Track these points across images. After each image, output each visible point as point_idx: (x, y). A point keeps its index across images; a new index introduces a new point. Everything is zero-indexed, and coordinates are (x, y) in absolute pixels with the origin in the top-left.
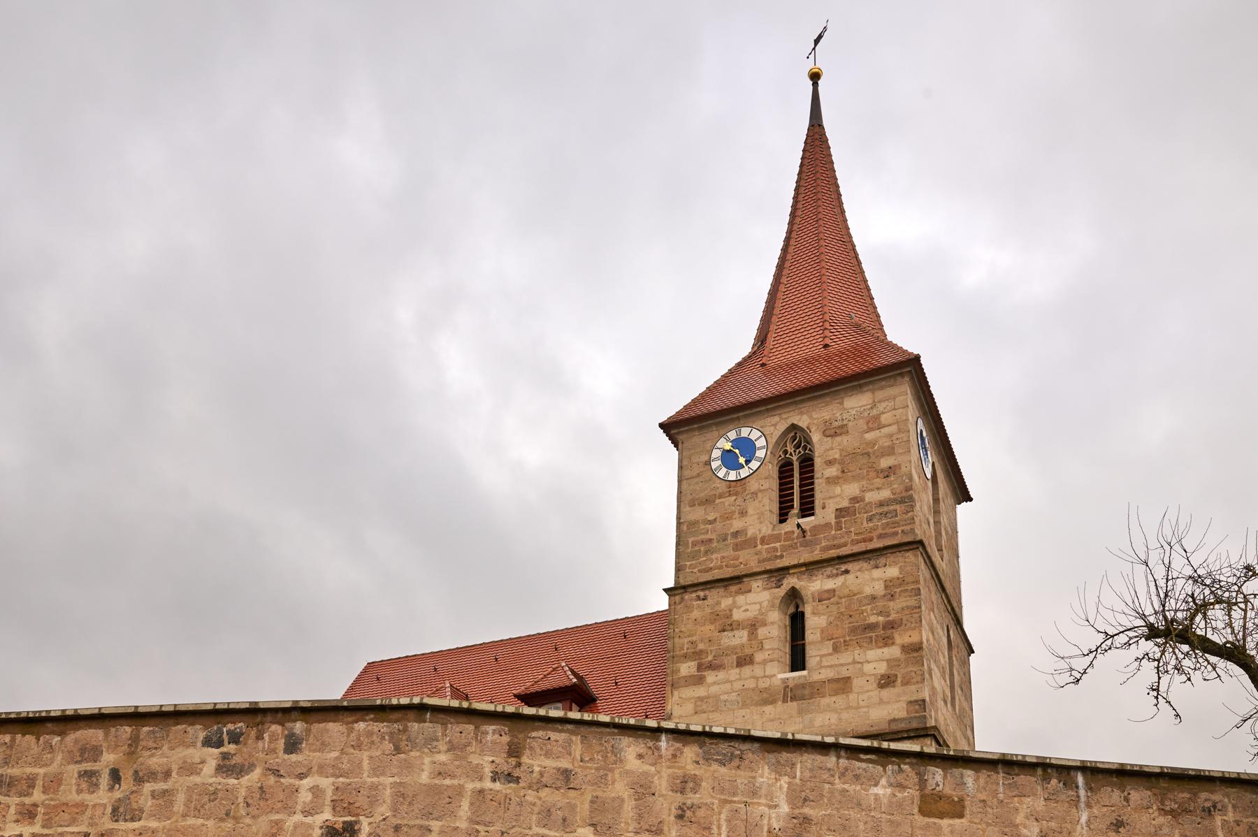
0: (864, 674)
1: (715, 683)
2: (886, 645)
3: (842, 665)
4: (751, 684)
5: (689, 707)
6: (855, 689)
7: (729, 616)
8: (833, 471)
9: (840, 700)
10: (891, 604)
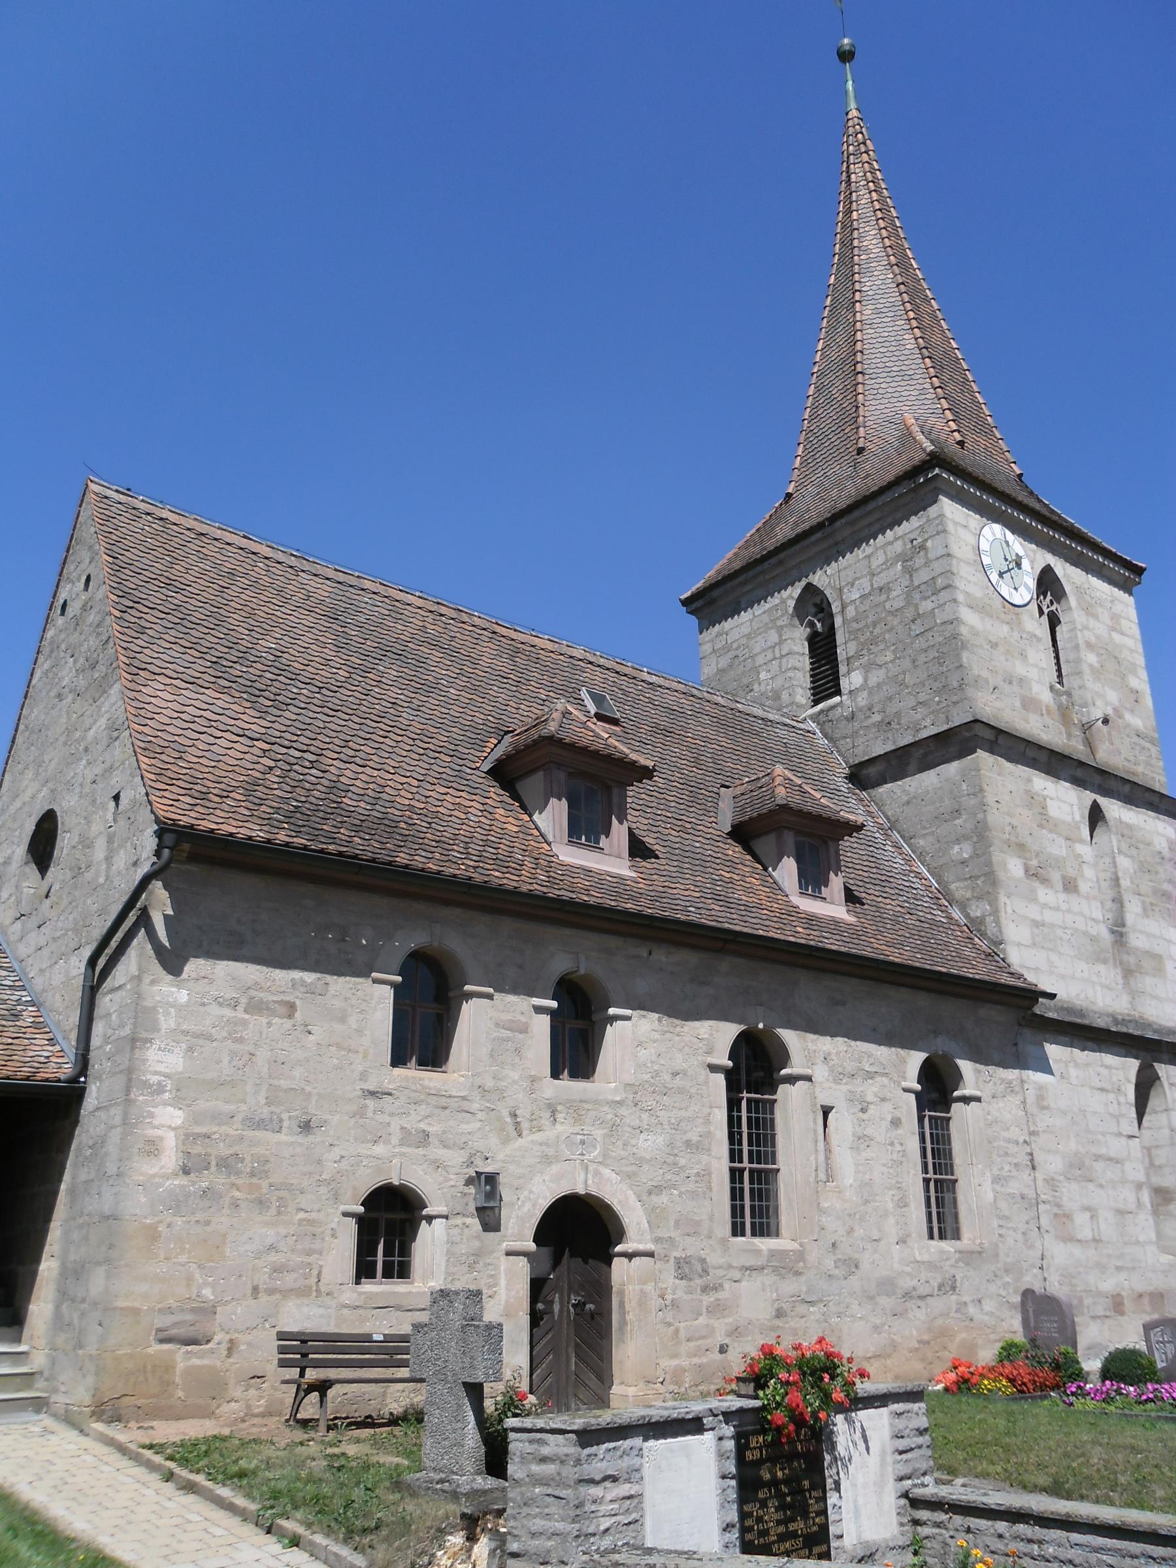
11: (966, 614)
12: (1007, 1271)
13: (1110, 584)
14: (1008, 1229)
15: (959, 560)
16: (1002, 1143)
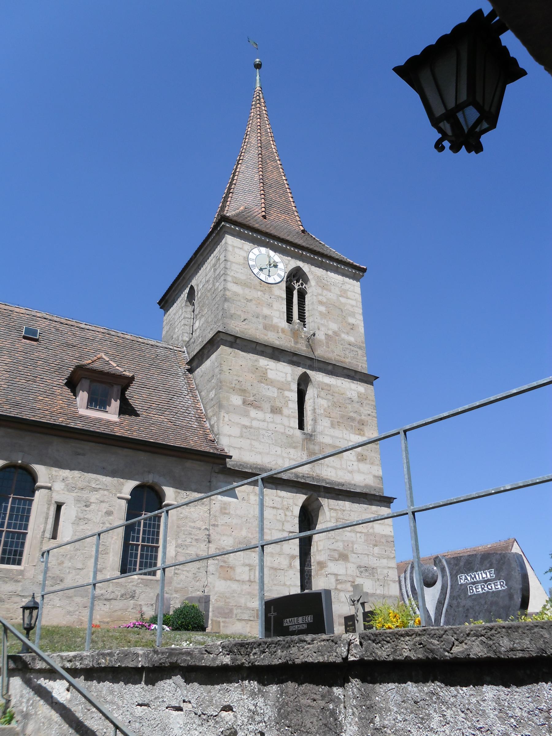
2: (360, 434)
3: (337, 438)
4: (280, 428)
5: (236, 431)
7: (265, 373)
10: (362, 409)
11: (231, 286)
12: (176, 591)
13: (343, 276)
14: (183, 571)
15: (232, 262)
16: (188, 529)
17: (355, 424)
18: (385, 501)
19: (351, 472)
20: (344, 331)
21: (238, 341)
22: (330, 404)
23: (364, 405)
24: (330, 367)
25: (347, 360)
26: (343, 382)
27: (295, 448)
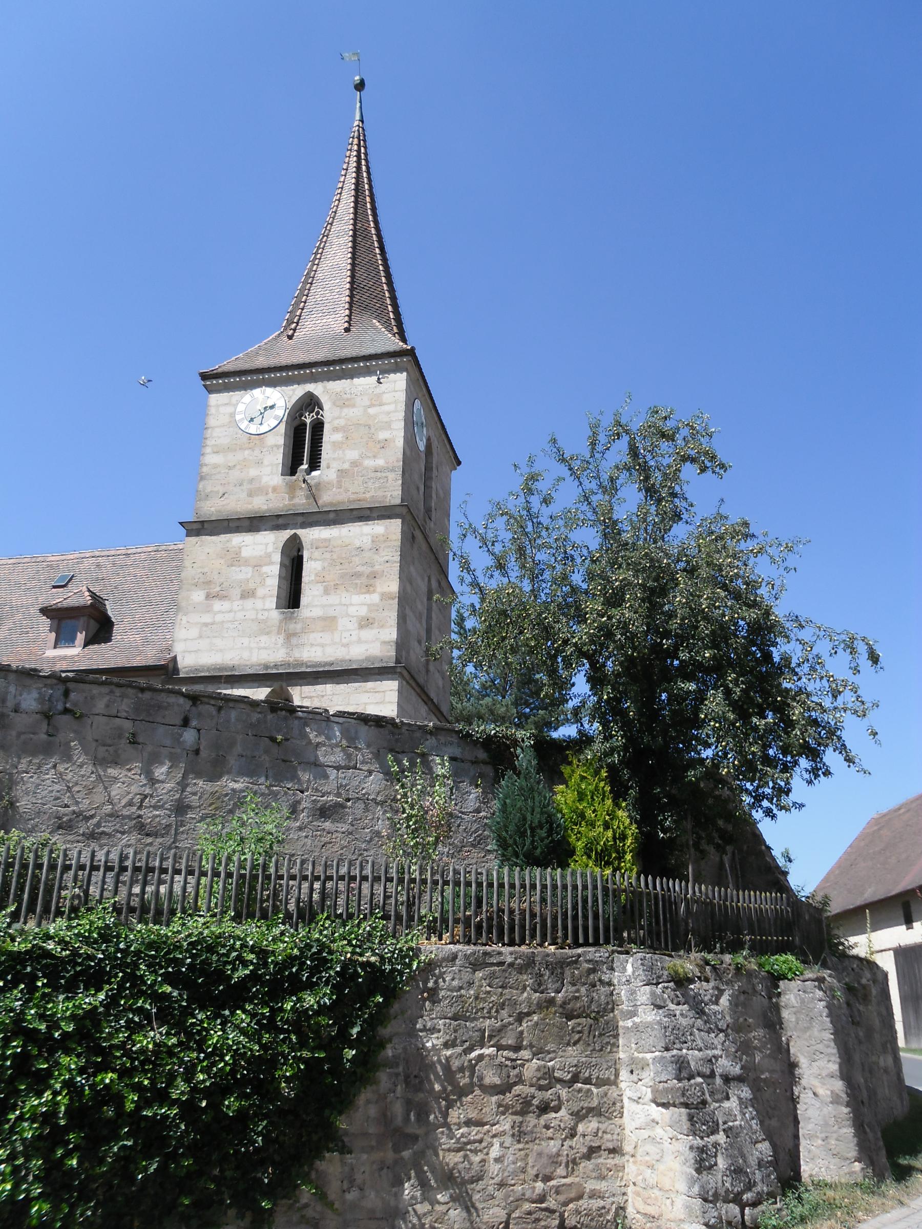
0: (348, 615)
1: (220, 612)
2: (368, 592)
3: (331, 605)
4: (251, 615)
5: (194, 632)
6: (340, 628)
7: (238, 553)
8: (338, 437)
9: (326, 638)
10: (376, 557)
15: (213, 428)
17: (364, 580)
18: (388, 673)
19: (346, 645)
20: (370, 455)
21: (206, 525)
22: (326, 564)
23: (381, 550)
24: (332, 516)
25: (368, 495)
26: (350, 528)
27: (267, 633)
